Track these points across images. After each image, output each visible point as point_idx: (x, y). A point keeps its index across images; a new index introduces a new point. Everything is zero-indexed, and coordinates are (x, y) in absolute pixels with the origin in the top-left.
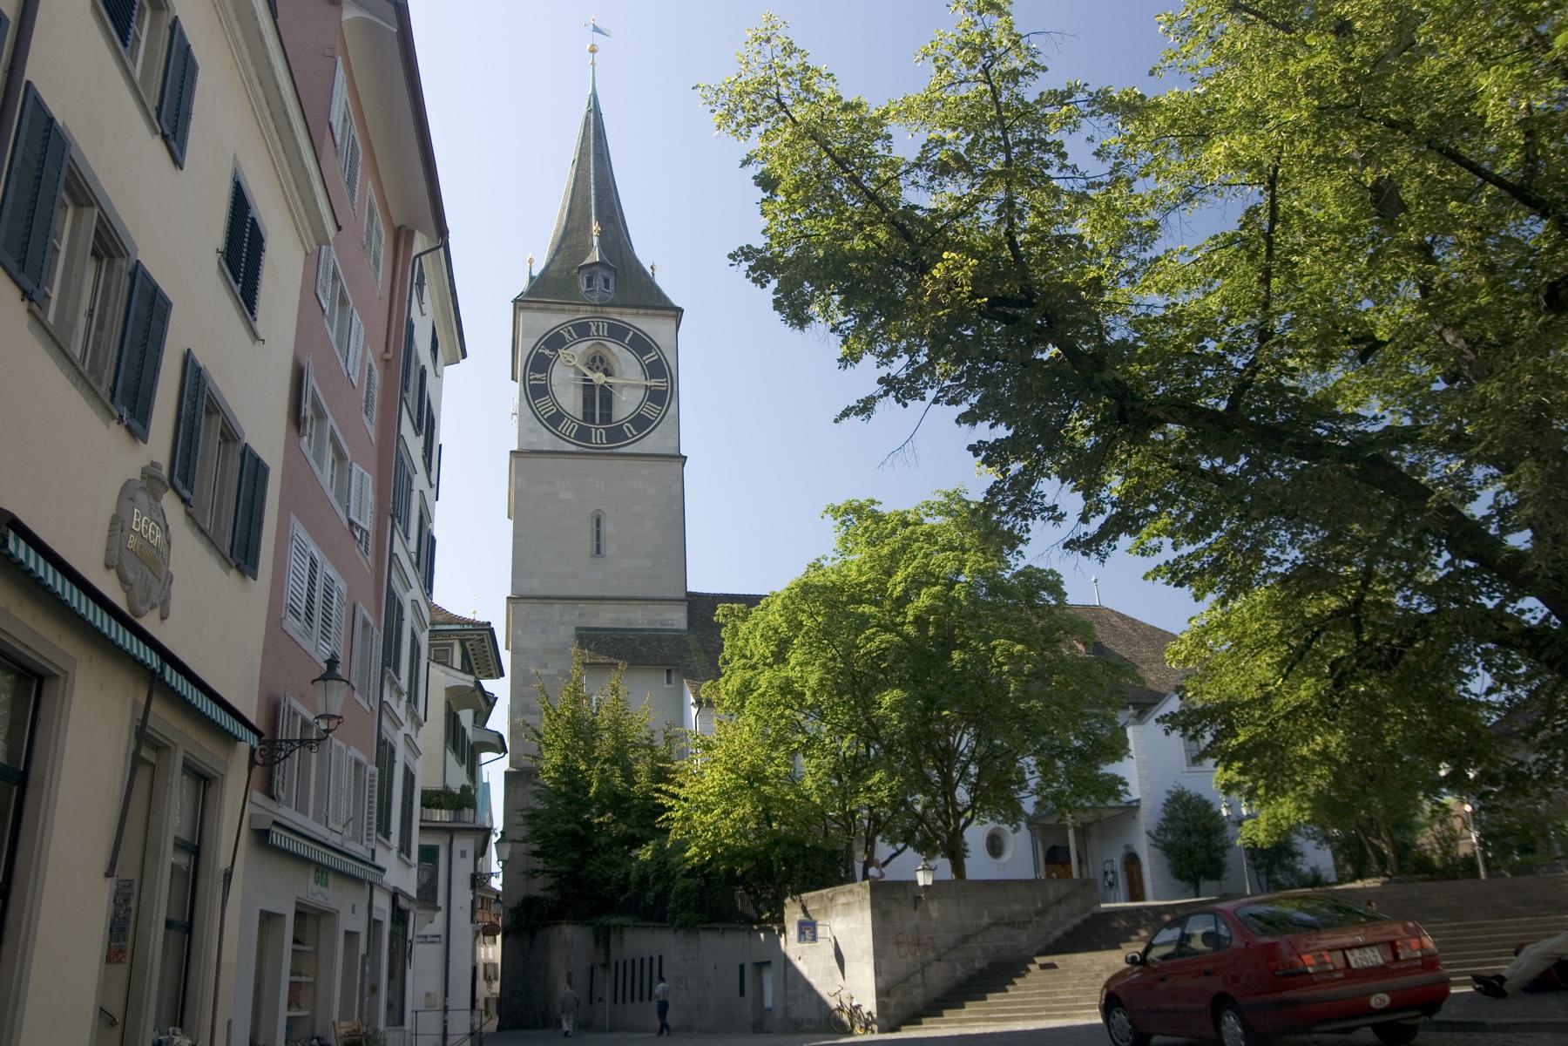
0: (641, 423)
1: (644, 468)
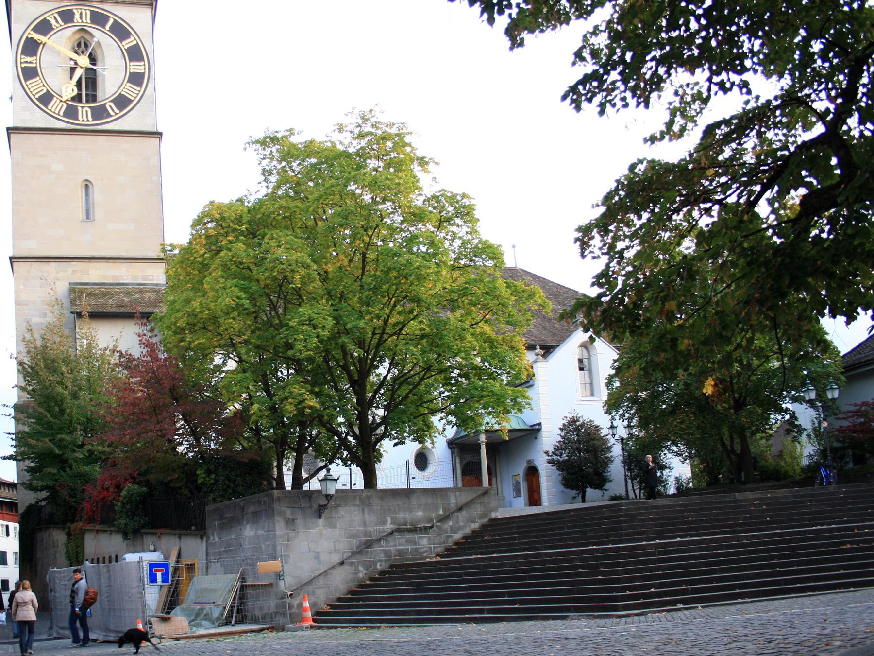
0: (122, 102)
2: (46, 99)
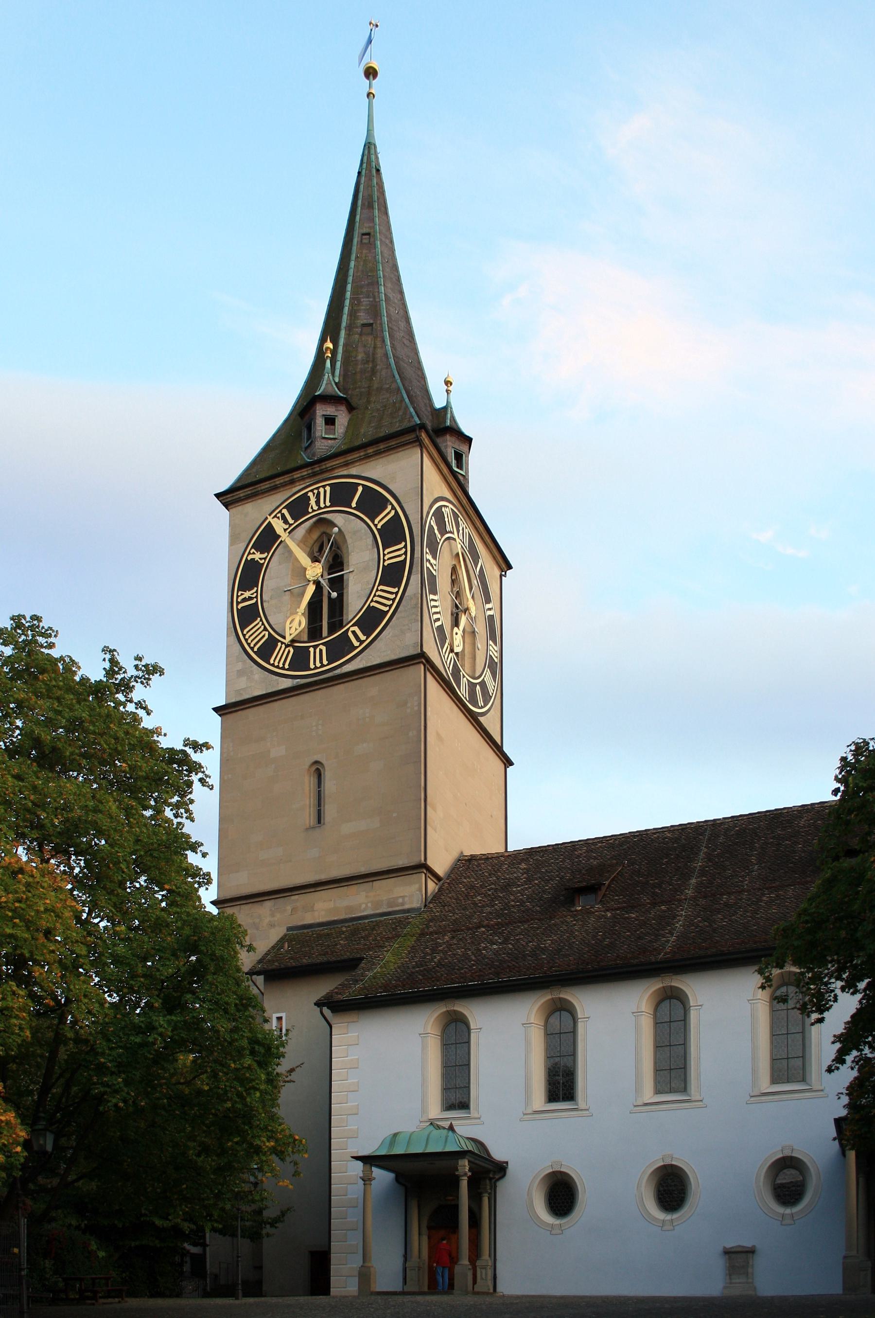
1: (372, 686)
2: (267, 650)
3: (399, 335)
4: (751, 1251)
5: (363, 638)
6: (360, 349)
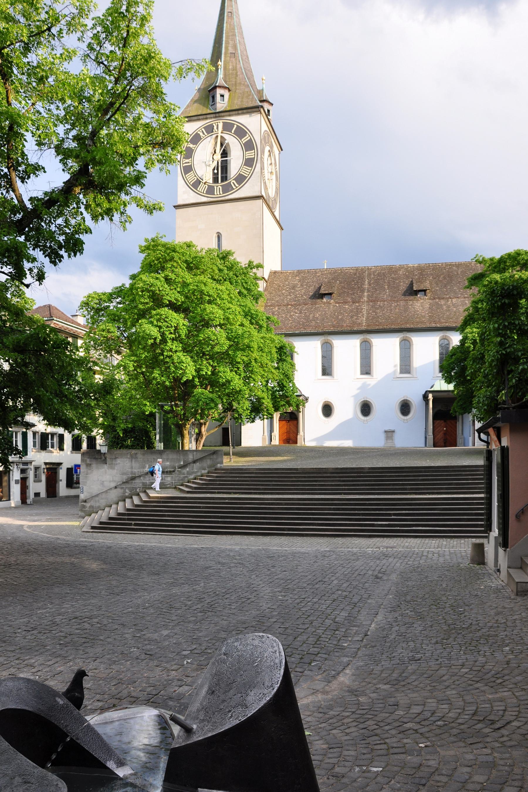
0: (241, 179)
3: (244, 58)
4: (393, 432)
5: (237, 185)
6: (230, 64)
